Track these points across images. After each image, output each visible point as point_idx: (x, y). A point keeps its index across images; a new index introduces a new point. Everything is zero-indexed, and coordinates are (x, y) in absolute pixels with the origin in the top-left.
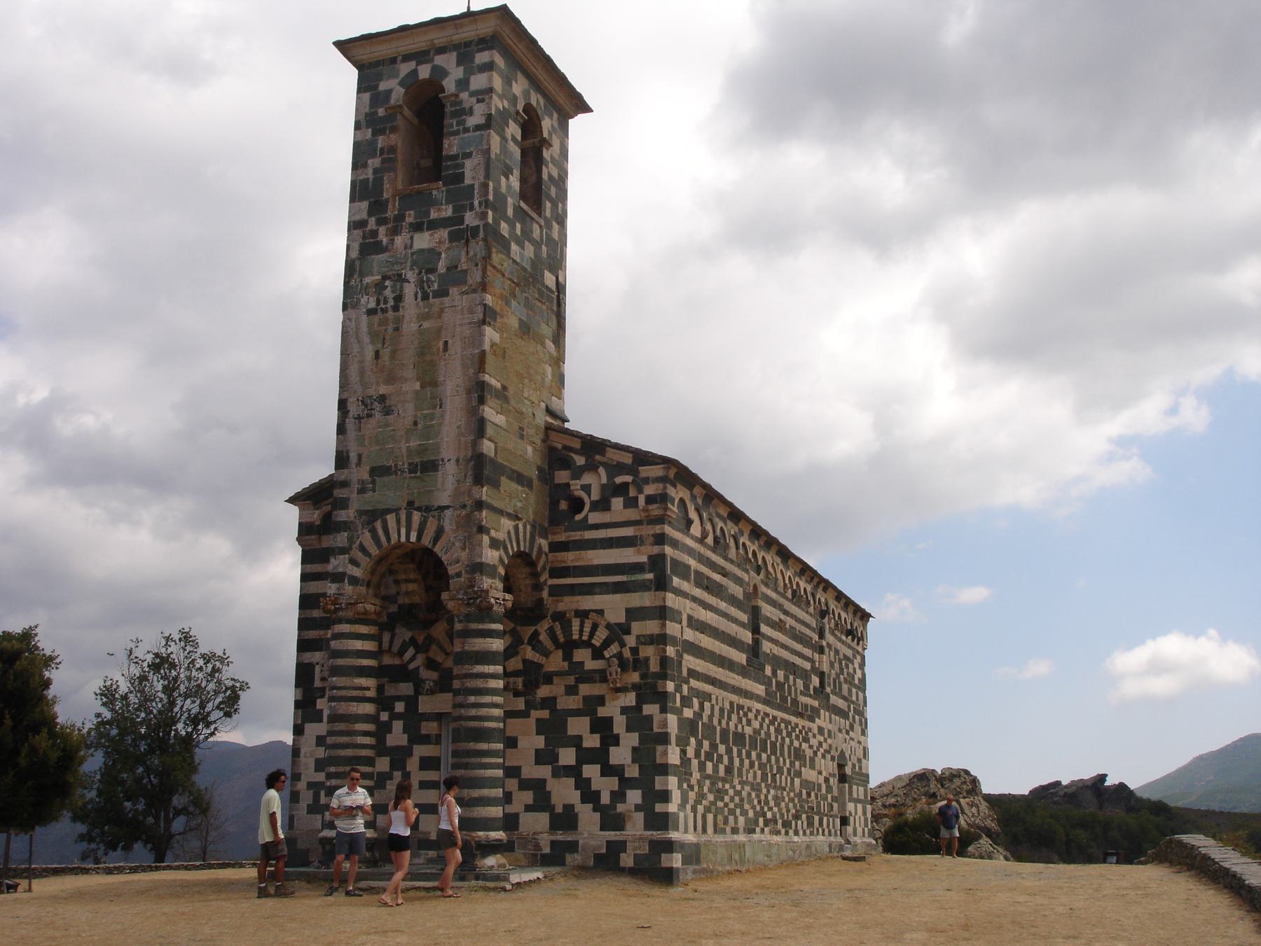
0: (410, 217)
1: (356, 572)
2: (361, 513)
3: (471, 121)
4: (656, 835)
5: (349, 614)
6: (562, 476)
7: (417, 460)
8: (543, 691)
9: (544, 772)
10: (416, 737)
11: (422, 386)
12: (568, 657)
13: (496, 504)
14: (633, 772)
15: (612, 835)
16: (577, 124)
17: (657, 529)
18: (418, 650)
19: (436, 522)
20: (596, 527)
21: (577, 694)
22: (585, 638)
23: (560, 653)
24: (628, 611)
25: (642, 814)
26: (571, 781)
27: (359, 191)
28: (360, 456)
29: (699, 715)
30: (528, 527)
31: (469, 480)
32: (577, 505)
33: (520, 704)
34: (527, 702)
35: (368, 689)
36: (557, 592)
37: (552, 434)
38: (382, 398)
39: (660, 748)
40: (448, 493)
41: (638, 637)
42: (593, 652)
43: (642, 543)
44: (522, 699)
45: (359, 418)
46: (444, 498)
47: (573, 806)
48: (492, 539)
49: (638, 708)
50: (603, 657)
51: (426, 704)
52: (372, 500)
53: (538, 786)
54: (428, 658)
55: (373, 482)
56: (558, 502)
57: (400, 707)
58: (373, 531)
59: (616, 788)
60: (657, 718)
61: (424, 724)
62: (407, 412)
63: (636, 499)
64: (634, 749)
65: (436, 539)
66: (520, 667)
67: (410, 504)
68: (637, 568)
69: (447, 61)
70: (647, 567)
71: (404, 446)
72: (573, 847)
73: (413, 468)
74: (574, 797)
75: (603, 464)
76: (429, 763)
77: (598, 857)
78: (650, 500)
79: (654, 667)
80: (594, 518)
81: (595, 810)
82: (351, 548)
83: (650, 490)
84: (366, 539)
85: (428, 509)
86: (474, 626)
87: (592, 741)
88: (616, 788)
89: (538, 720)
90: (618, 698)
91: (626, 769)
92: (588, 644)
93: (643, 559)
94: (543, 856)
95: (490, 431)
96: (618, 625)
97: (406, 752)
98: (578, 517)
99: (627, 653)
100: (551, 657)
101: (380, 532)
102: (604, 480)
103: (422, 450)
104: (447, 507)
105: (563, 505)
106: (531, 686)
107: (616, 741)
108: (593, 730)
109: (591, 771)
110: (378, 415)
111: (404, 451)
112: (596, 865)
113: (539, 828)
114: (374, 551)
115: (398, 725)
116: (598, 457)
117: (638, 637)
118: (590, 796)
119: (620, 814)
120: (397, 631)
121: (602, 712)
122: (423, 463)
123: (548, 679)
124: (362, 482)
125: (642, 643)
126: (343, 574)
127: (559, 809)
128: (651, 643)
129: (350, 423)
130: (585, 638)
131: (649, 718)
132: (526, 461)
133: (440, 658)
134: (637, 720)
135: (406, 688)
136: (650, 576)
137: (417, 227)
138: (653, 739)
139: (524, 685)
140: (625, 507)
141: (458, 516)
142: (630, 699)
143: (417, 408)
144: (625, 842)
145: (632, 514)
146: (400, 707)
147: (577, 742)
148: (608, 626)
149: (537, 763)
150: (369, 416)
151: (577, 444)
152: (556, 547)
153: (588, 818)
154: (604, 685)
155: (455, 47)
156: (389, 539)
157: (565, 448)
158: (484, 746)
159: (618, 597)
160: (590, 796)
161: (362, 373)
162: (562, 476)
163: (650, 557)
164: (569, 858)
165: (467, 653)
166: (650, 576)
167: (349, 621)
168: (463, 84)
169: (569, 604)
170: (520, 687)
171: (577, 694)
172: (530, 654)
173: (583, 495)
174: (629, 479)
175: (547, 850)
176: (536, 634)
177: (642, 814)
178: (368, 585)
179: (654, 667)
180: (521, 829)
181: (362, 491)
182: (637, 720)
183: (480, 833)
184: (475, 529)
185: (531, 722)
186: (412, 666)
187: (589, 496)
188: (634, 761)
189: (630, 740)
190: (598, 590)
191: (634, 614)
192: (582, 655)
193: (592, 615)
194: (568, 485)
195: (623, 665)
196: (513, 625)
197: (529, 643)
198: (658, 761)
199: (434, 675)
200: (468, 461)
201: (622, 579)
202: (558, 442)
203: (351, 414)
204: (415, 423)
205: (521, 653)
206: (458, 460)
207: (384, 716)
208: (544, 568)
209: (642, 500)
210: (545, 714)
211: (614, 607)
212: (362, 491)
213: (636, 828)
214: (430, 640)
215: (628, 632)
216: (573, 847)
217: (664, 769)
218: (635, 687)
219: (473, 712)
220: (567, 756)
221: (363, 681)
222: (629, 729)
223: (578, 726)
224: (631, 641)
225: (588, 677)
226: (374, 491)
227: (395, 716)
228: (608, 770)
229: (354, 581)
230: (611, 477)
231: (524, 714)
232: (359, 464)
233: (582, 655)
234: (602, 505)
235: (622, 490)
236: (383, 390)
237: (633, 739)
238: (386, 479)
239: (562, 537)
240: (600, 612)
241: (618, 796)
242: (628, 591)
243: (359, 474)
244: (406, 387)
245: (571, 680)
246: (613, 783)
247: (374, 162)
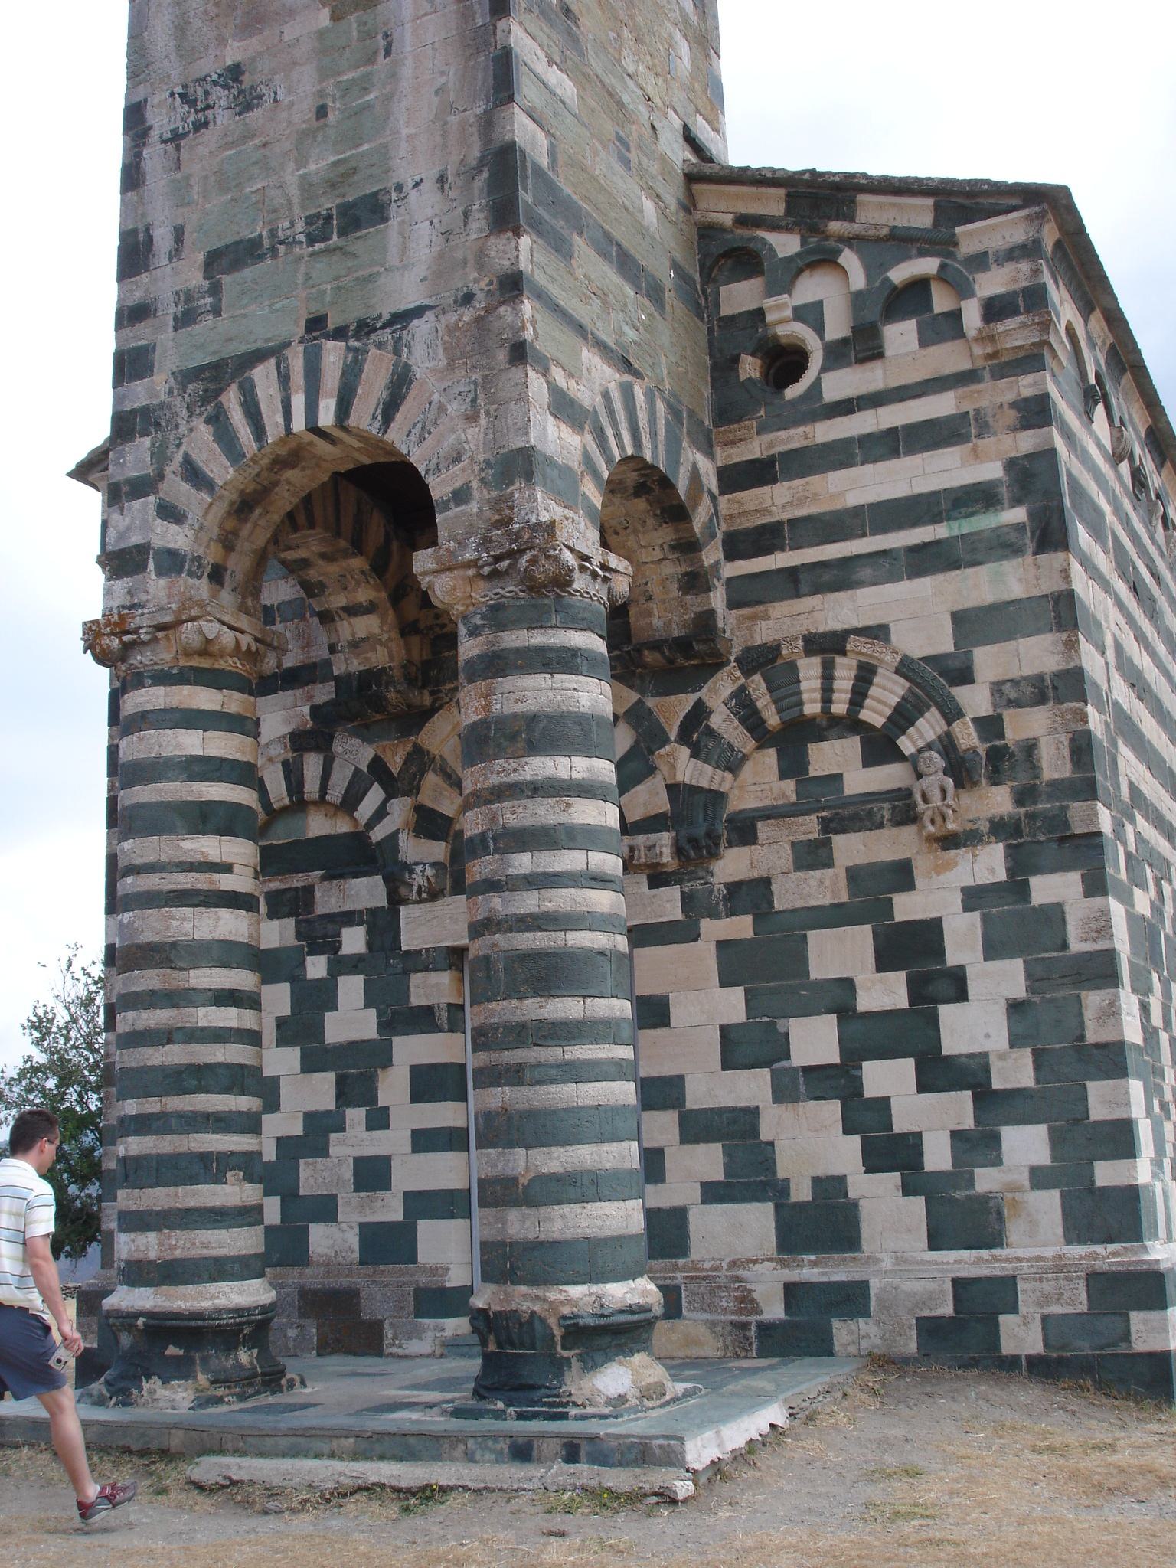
1: (176, 537)
2: (186, 377)
4: (1109, 1256)
5: (162, 656)
6: (739, 296)
7: (328, 204)
8: (733, 865)
9: (751, 1087)
10: (401, 1017)
11: (336, 17)
12: (793, 766)
13: (554, 290)
14: (1015, 1072)
15: (967, 1262)
17: (1026, 386)
18: (393, 787)
19: (389, 358)
20: (846, 407)
21: (828, 863)
22: (839, 708)
23: (770, 757)
25: (1055, 1195)
26: (832, 1110)
28: (179, 233)
29: (1157, 909)
30: (660, 406)
31: (479, 222)
32: (786, 362)
33: (668, 904)
34: (687, 900)
35: (227, 868)
36: (744, 593)
37: (697, 187)
38: (235, 72)
39: (1093, 1000)
40: (421, 270)
41: (997, 688)
43: (984, 429)
44: (673, 893)
45: (176, 137)
46: (406, 289)
47: (841, 1180)
48: (556, 392)
49: (1016, 887)
50: (898, 756)
51: (425, 926)
52: (210, 341)
53: (735, 1128)
54: (419, 809)
55: (215, 290)
56: (735, 360)
57: (354, 940)
58: (218, 420)
59: (968, 1123)
60: (1078, 909)
61: (416, 979)
62: (297, 90)
63: (956, 316)
64: (1015, 1007)
65: (390, 409)
66: (663, 804)
67: (316, 324)
68: (981, 497)
70: (1004, 493)
71: (291, 177)
72: (851, 1299)
73: (318, 229)
74: (844, 1154)
75: (850, 241)
76: (431, 1083)
77: (931, 1329)
78: (994, 310)
79: (1054, 764)
80: (839, 384)
81: (907, 1190)
82: (161, 476)
83: (993, 283)
85: (365, 328)
86: (516, 639)
87: (885, 993)
88: (968, 1123)
89: (722, 945)
90: (949, 866)
91: (995, 1066)
92: (851, 724)
93: (992, 471)
94: (765, 1328)
95: (527, 91)
97: (378, 1055)
98: (792, 392)
99: (967, 736)
100: (747, 771)
101: (237, 417)
102: (858, 280)
103: (341, 175)
104: (418, 312)
105: (750, 368)
106: (696, 852)
107: (957, 987)
108: (883, 964)
109: (888, 1078)
110: (222, 118)
111: (294, 191)
112: (926, 1353)
113: (746, 1247)
114: (220, 470)
115: (351, 988)
116: (835, 226)
117: (997, 688)
118: (889, 1151)
119: (985, 1199)
120: (338, 747)
121: (907, 907)
122: (345, 209)
123: (744, 831)
124: (188, 296)
125: (1011, 703)
126: (143, 549)
127: (801, 1192)
128: (1040, 699)
129: (154, 156)
130: (839, 708)
131: (1054, 914)
132: (643, 232)
133: (448, 806)
135: (366, 891)
136: (1017, 515)
138: (1065, 974)
139: (679, 851)
140: (924, 343)
141: (451, 330)
142: (990, 864)
143: (323, 74)
144: (1010, 1282)
145: (949, 358)
146: (354, 940)
147: (839, 998)
148: (906, 668)
149: (727, 1065)
150: (201, 126)
151: (773, 204)
152: (735, 478)
153: (889, 1213)
154: (908, 832)
156: (259, 431)
157: (742, 220)
158: (569, 1008)
159: (925, 585)
160: (889, 1151)
161: (181, 29)
163: (1011, 464)
164: (843, 1331)
165: (501, 721)
166: (1017, 515)
167: (163, 678)
170: (666, 856)
171: (828, 863)
172: (686, 768)
173: (802, 332)
174: (928, 266)
175: (774, 1311)
177: (1055, 1195)
178: (217, 575)
179: (1054, 764)
180: (697, 1251)
181: (186, 319)
183: (576, 1291)
184: (502, 356)
185: (703, 954)
186: (377, 834)
187: (819, 329)
188: (1015, 1042)
189: (998, 982)
190: (866, 573)
191: (971, 625)
193: (853, 643)
194: (759, 313)
195: (961, 770)
196: (634, 696)
197: (684, 737)
198: (1091, 1037)
199: (438, 850)
200: (472, 173)
201: (931, 538)
202: (722, 207)
203: (155, 135)
204: (322, 112)
205: (664, 769)
206: (442, 179)
207: (316, 967)
208: (709, 527)
209: (972, 316)
210: (741, 927)
211: (916, 615)
212: (186, 319)
213: (1037, 1238)
214: (420, 760)
216: (851, 1299)
217: (1112, 1060)
218: (1000, 828)
219: (529, 902)
220: (815, 1040)
221: (209, 847)
222: (993, 950)
223: (841, 954)
224: (976, 700)
226: (216, 311)
227: (342, 966)
228: (938, 1072)
229: (172, 562)
230: (875, 268)
231: (683, 932)
232: (176, 253)
233: (834, 755)
234: (863, 345)
235: (911, 299)
236: (234, 53)
238: (248, 273)
239: (755, 448)
240: (878, 633)
241: (977, 1145)
242: (955, 565)
243: (176, 276)
244: (291, 31)
245: (809, 827)
246: (957, 1108)
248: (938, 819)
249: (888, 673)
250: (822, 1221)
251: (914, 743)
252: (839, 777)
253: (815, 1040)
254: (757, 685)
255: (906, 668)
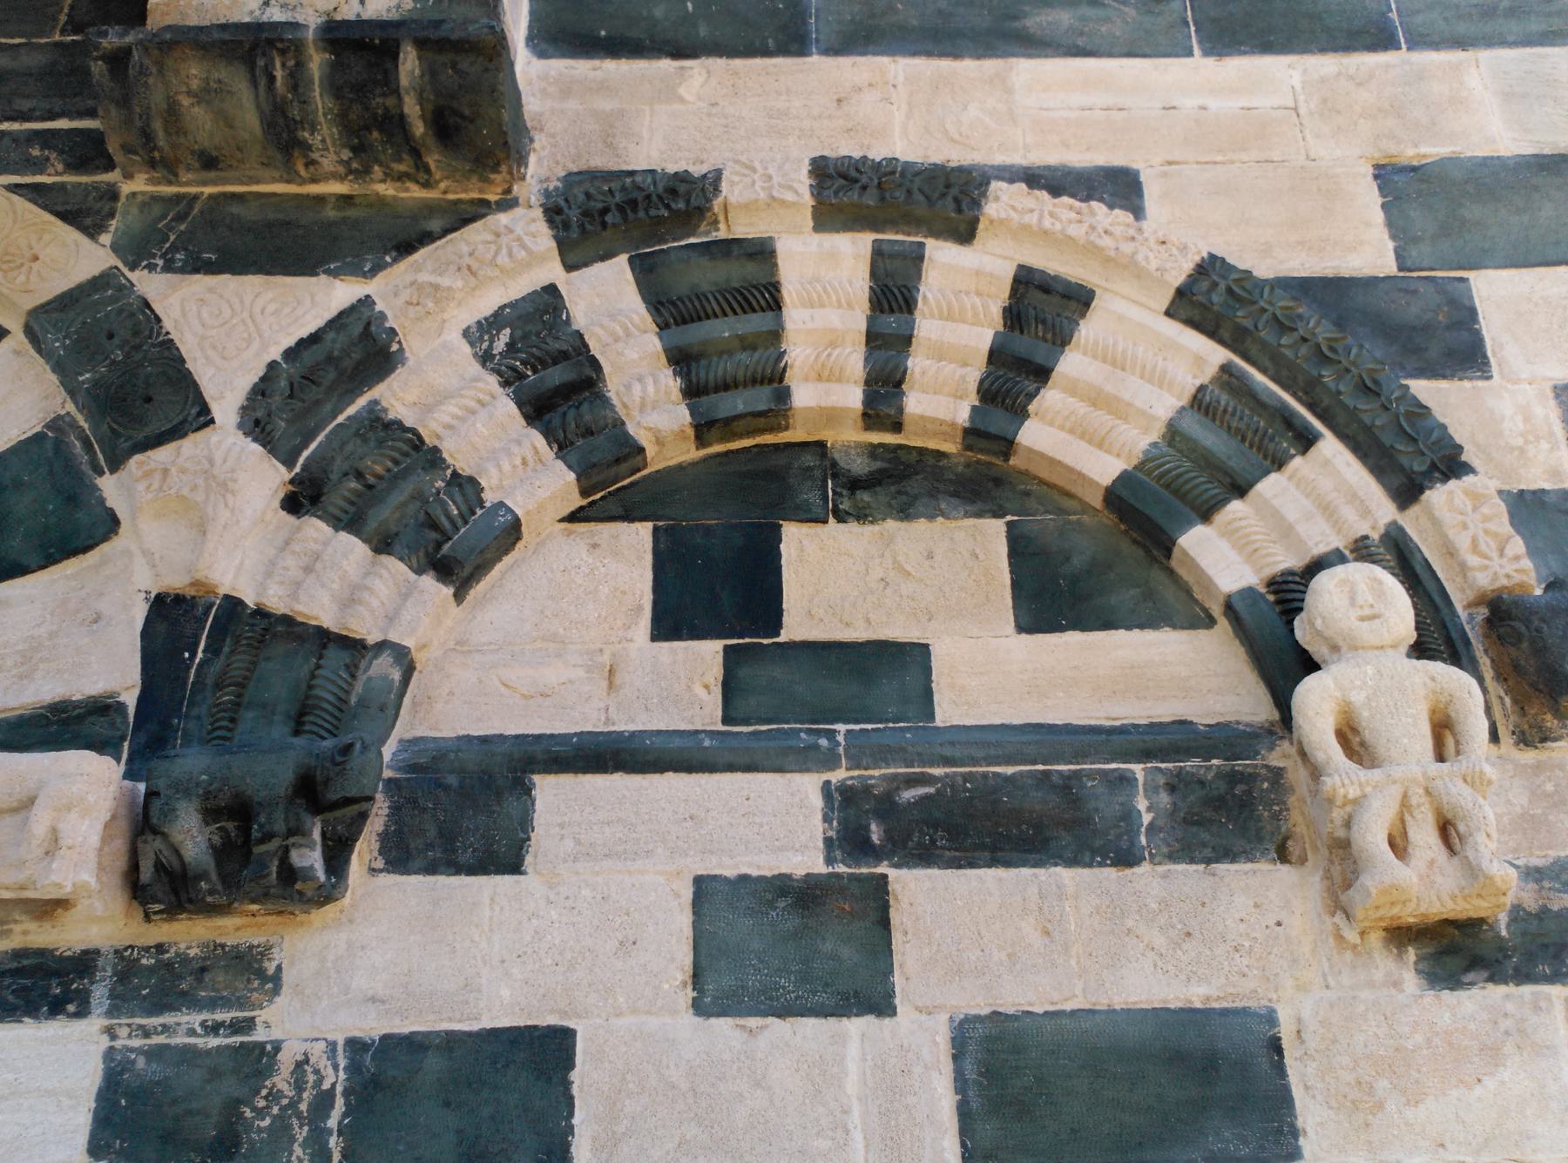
22: (940, 398)
23: (626, 556)
24: (1400, 183)
42: (1024, 553)
96: (1330, 293)
100: (510, 589)
123: (470, 813)
148: (1212, 299)
169: (745, 126)
171: (871, 997)
176: (361, 349)
193: (1003, 202)
215: (1465, 354)
225: (1025, 810)
245: (777, 822)
248: (1424, 836)
249: (1135, 313)
251: (1251, 554)
252: (913, 658)
254: (608, 305)
255: (1212, 299)
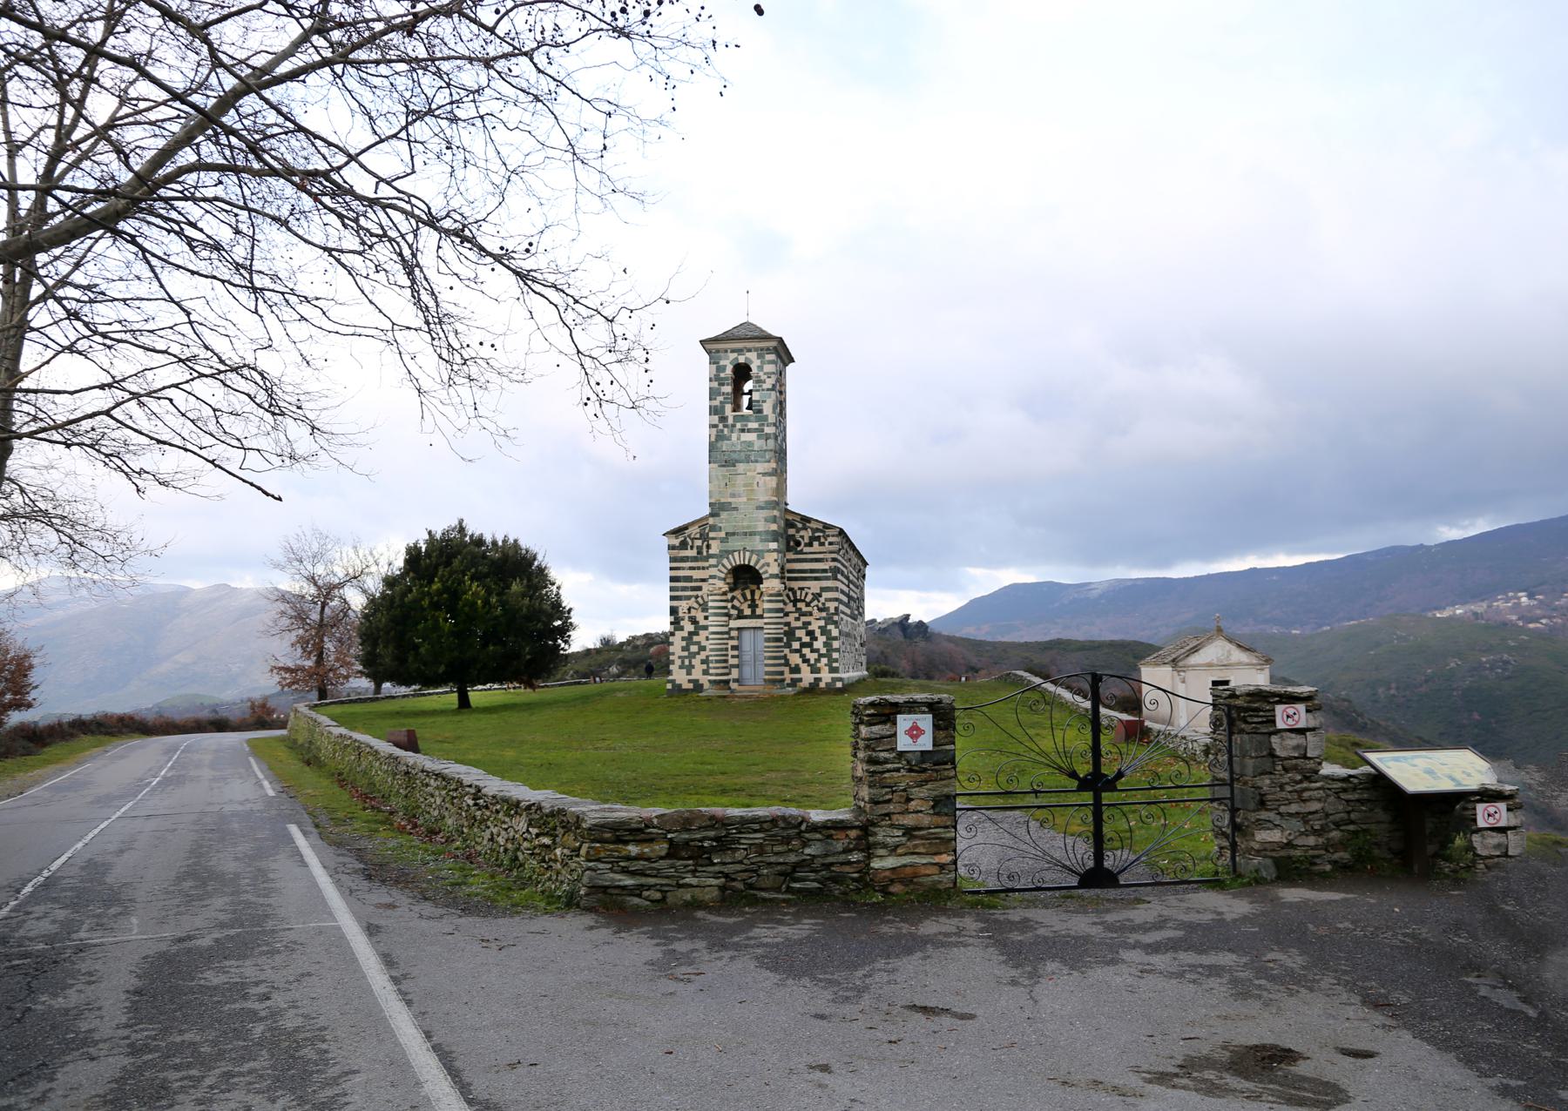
0: (739, 426)
3: (765, 386)
6: (791, 531)
9: (787, 651)
14: (823, 651)
16: (790, 368)
27: (714, 411)
32: (798, 544)
68: (825, 571)
69: (752, 356)
76: (734, 648)
80: (807, 549)
84: (725, 561)
87: (806, 639)
118: (806, 661)
134: (824, 631)
137: (743, 431)
142: (822, 623)
145: (822, 549)
155: (756, 349)
160: (806, 661)
162: (791, 531)
168: (760, 368)
182: (824, 631)
191: (823, 589)
192: (799, 605)
195: (820, 610)
211: (815, 587)
223: (800, 633)
225: (805, 614)
228: (813, 651)
234: (810, 544)
237: (823, 639)
241: (818, 660)
246: (815, 655)
247: (721, 398)
250: (796, 670)
253: (796, 645)
